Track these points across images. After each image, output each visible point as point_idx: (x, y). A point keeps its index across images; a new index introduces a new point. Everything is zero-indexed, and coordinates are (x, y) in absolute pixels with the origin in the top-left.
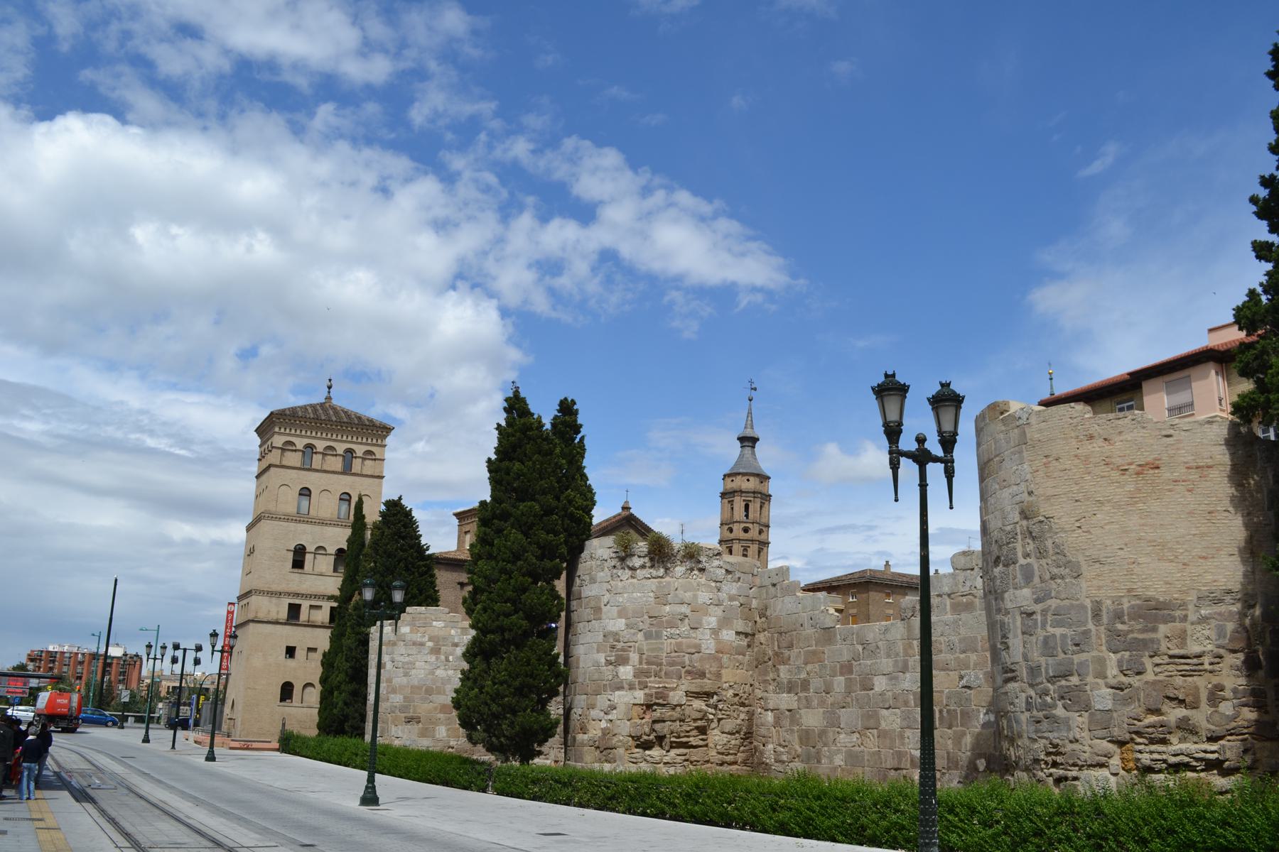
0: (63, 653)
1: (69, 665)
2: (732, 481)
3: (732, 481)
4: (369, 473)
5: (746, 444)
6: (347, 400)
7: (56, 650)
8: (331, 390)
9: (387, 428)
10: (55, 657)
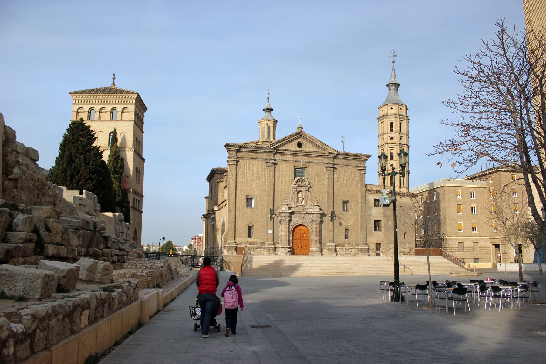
2: (383, 110)
3: (383, 110)
8: (115, 80)
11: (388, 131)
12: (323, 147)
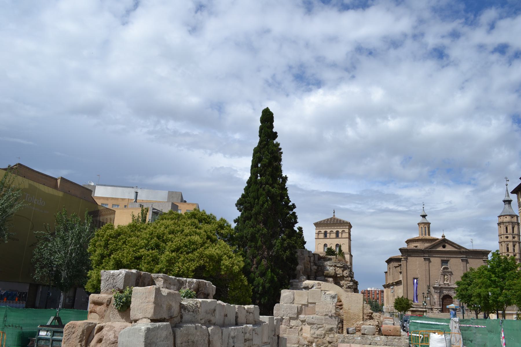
0: (372, 291)
1: (374, 295)
4: (344, 237)
5: (506, 203)
6: (339, 216)
7: (370, 290)
9: (347, 223)
10: (369, 292)
11: (504, 233)
12: (460, 247)
